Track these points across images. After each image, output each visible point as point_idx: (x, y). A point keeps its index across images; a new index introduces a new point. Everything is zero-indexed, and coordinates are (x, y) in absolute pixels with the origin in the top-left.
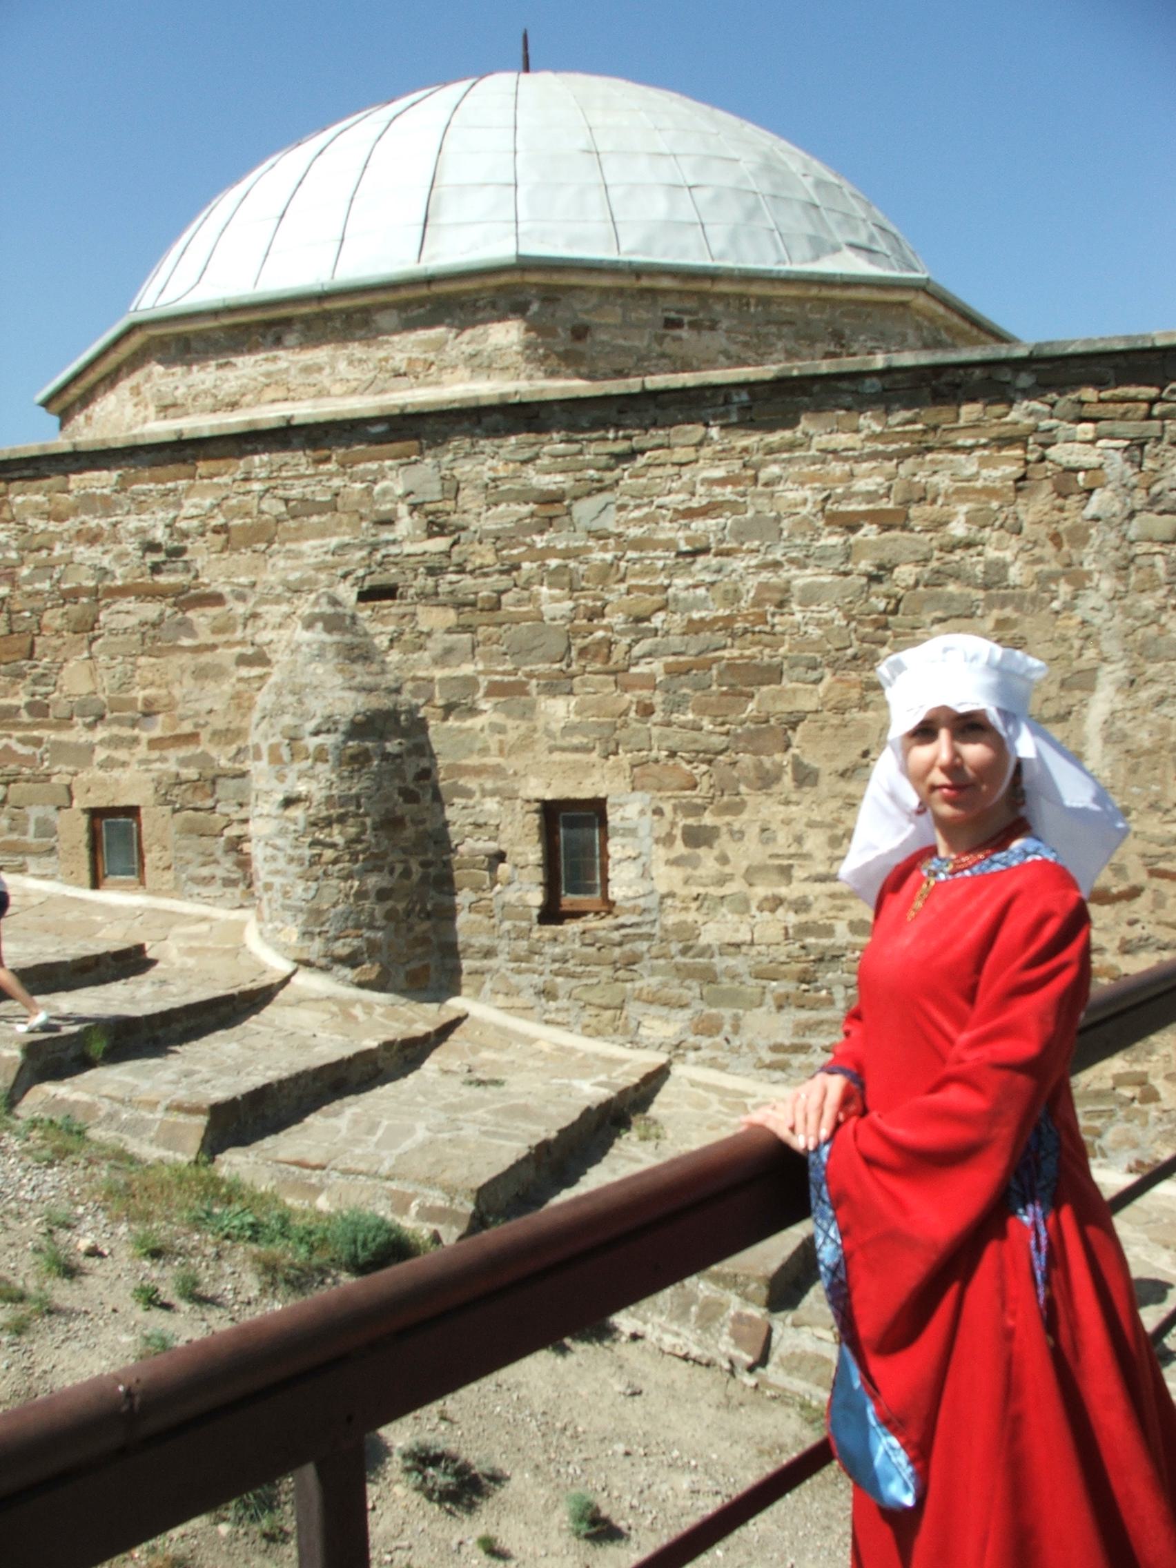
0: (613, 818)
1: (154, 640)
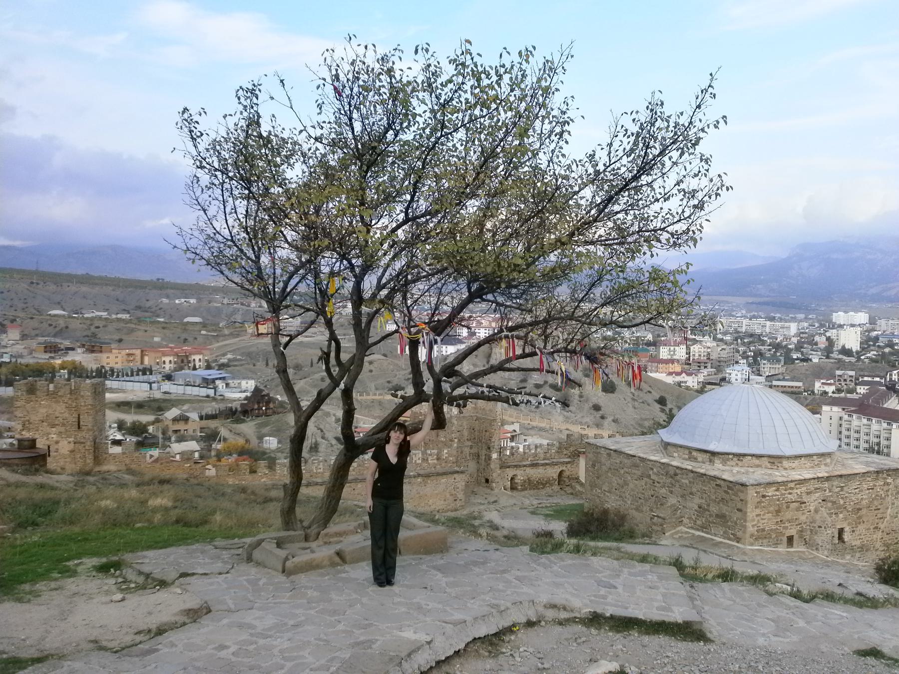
0: (845, 530)
1: (798, 509)
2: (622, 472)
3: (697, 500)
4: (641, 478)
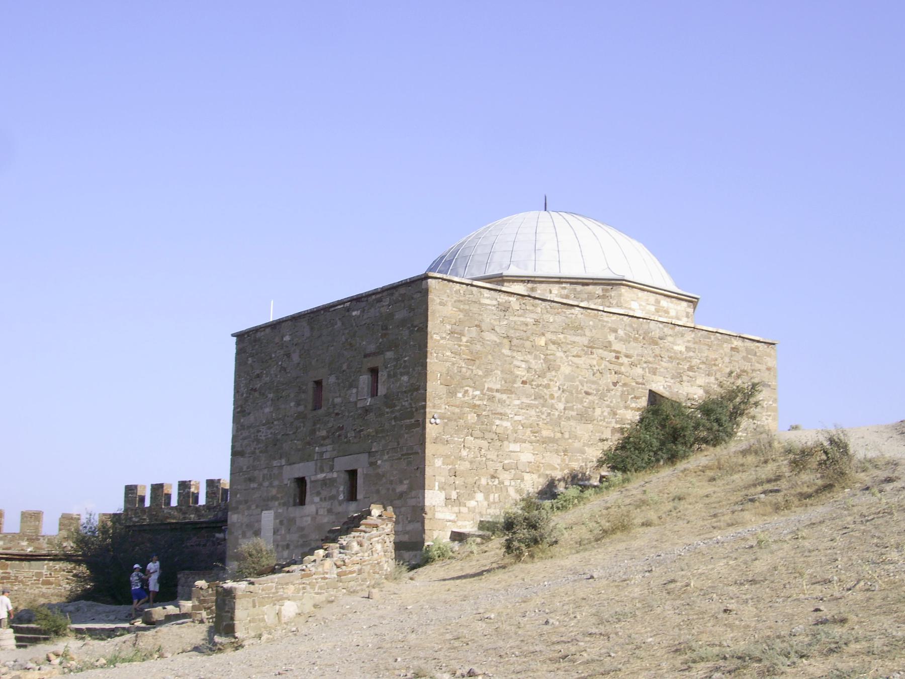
2: (542, 342)
3: (701, 380)
4: (590, 348)
